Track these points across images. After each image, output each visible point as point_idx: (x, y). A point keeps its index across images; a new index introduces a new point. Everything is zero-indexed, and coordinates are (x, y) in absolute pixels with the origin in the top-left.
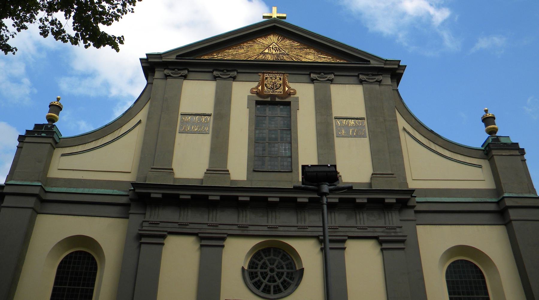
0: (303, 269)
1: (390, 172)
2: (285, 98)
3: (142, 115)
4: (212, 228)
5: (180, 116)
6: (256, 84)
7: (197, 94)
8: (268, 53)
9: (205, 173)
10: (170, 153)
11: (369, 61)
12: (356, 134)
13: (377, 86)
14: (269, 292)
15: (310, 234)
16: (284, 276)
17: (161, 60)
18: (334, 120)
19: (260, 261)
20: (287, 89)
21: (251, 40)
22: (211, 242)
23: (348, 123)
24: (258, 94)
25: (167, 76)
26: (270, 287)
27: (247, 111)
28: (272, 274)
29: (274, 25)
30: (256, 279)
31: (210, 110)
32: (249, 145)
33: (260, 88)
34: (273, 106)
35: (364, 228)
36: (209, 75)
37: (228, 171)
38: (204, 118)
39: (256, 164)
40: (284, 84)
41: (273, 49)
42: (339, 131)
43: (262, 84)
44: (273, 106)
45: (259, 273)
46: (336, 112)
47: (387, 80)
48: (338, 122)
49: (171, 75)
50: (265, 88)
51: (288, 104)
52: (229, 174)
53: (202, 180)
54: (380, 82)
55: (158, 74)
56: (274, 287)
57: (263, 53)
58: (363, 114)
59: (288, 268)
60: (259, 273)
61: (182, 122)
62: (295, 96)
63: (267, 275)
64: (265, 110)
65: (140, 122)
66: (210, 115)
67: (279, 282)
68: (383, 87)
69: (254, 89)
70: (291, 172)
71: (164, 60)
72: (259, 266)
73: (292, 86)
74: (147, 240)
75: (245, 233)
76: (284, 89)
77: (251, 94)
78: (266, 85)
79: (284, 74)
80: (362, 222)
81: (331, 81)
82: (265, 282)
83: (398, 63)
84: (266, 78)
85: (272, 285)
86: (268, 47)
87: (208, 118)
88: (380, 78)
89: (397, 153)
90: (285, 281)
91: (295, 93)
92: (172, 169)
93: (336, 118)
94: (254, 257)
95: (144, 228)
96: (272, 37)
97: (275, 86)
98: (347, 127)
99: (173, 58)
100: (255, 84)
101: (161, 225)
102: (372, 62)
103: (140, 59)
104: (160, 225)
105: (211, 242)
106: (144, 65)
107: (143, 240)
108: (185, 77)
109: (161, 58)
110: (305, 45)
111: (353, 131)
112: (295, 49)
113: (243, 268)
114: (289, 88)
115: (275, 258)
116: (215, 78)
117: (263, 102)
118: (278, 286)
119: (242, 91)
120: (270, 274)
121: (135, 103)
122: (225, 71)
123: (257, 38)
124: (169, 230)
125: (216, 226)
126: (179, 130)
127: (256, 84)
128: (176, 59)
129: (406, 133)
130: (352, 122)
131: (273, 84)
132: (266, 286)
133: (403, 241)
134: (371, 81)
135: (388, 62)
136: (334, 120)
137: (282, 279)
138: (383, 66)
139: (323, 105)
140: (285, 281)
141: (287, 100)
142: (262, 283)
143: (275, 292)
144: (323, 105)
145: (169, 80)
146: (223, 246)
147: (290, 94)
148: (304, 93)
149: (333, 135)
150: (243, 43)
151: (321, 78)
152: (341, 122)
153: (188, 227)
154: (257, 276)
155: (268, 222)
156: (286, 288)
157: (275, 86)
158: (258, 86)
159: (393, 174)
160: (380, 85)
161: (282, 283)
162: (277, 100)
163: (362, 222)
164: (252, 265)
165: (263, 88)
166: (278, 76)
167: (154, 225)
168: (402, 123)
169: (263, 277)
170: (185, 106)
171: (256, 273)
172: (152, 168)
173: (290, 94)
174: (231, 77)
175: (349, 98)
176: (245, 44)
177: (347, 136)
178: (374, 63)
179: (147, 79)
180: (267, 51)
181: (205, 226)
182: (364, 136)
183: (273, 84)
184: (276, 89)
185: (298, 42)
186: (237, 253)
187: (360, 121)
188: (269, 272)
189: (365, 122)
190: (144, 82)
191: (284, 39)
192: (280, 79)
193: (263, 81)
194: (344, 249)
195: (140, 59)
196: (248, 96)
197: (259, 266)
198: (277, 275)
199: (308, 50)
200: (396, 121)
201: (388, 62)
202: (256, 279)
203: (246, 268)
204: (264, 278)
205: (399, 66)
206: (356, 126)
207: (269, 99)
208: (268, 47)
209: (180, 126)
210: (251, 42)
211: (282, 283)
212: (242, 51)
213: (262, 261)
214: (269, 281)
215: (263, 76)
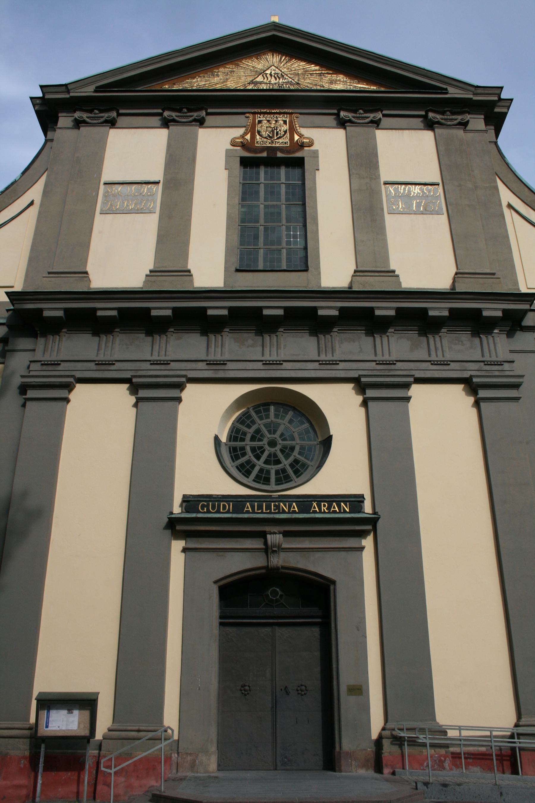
0: (331, 437)
1: (488, 271)
2: (294, 152)
3: (35, 193)
4: (158, 367)
5: (102, 187)
6: (242, 131)
7: (134, 150)
8: (261, 83)
9: (147, 276)
10: (84, 246)
11: (446, 89)
12: (425, 209)
13: (460, 133)
14: (267, 481)
15: (342, 374)
16: (296, 453)
17: (67, 96)
18: (383, 187)
19: (249, 427)
20: (296, 138)
21: (231, 63)
22: (155, 392)
23: (409, 191)
24: (243, 146)
25: (78, 124)
26: (268, 472)
27: (225, 174)
28: (273, 450)
29: (274, 35)
30: (243, 460)
31: (158, 175)
32: (228, 228)
33: (248, 137)
34: (273, 174)
35: (446, 363)
36: (156, 120)
37: (189, 271)
38: (146, 188)
39: (243, 260)
40: (292, 130)
41: (271, 75)
42: (393, 204)
43: (252, 130)
44: (273, 174)
45: (248, 449)
46: (386, 173)
47: (477, 122)
48: (391, 189)
49: (88, 120)
50: (258, 137)
51: (299, 163)
52: (192, 276)
53: (142, 288)
54: (464, 125)
55: (65, 120)
56: (277, 472)
58: (437, 179)
59: (302, 439)
60: (248, 449)
61: (106, 195)
62: (312, 148)
63: (263, 452)
64: (258, 174)
65: (32, 203)
66: (157, 183)
67: (286, 463)
68: (470, 135)
69: (238, 138)
70: (306, 270)
71: (72, 94)
72: (248, 437)
73: (307, 133)
75: (221, 375)
76: (292, 138)
77: (232, 148)
78: (259, 132)
79: (292, 113)
80: (440, 353)
81: (376, 123)
82: (260, 464)
83: (497, 91)
84: (260, 122)
85: (273, 469)
86: (262, 73)
87: (154, 187)
88: (467, 117)
89: (501, 241)
90: (296, 461)
91: (311, 144)
92: (86, 273)
93: (385, 183)
95: (32, 373)
96: (269, 57)
97: (274, 133)
98: (408, 197)
99: (89, 91)
100: (238, 132)
101: (63, 366)
102: (451, 90)
103: (31, 98)
104: (60, 368)
105: (155, 392)
106: (37, 108)
107: (31, 394)
108: (112, 123)
109: (68, 92)
110: (328, 68)
111: (418, 205)
112: (311, 74)
113: (217, 439)
114: (301, 136)
115: (279, 421)
116: (166, 124)
117: (252, 161)
118: (284, 471)
119: (215, 144)
120: (268, 451)
121: (23, 173)
122: (185, 110)
123: (243, 59)
124: (78, 375)
125: (167, 363)
126: (101, 210)
127: (242, 131)
128: (95, 91)
129: (513, 211)
130: (416, 190)
131: (273, 131)
132: (261, 470)
134: (449, 123)
135: (479, 91)
136: (383, 187)
137: (291, 459)
138: (471, 96)
139: (363, 164)
140: (296, 461)
141: (298, 155)
142: (254, 466)
143: (279, 482)
145: (84, 130)
147: (302, 146)
148: (328, 144)
149: (383, 209)
150: (218, 67)
151: (358, 118)
152: (396, 190)
153: (112, 367)
154: (244, 454)
155: (263, 355)
156: (297, 473)
157: (274, 133)
158: (245, 134)
159: (494, 274)
160: (465, 130)
161: (291, 465)
162: (279, 155)
163: (440, 353)
164: (235, 434)
165: (253, 137)
166: (281, 119)
167: (51, 368)
168: (506, 196)
169: (255, 456)
170: (110, 171)
171: (243, 448)
172: (49, 273)
173: (302, 146)
174: (195, 120)
175: (408, 152)
176: (222, 69)
177: (408, 212)
178: (453, 93)
179: (45, 135)
180: (260, 79)
181: (147, 366)
182: (439, 213)
183: (273, 131)
184: (278, 139)
185: (316, 65)
186: (206, 412)
187: (430, 187)
188: (267, 447)
189: (440, 189)
190: (42, 139)
191: (290, 61)
192: (285, 122)
193: (253, 126)
194: (408, 399)
195: (31, 98)
196: (227, 151)
197: (248, 437)
198: (282, 451)
199: (334, 77)
200: (496, 188)
201: (479, 91)
202: (243, 460)
203: (224, 439)
204: (258, 458)
205: (500, 99)
206: (424, 196)
207: (265, 154)
208: (262, 73)
209: (103, 203)
210: (231, 66)
211: (291, 465)
212: (216, 80)
213: (254, 428)
214: (266, 462)
215: (254, 119)
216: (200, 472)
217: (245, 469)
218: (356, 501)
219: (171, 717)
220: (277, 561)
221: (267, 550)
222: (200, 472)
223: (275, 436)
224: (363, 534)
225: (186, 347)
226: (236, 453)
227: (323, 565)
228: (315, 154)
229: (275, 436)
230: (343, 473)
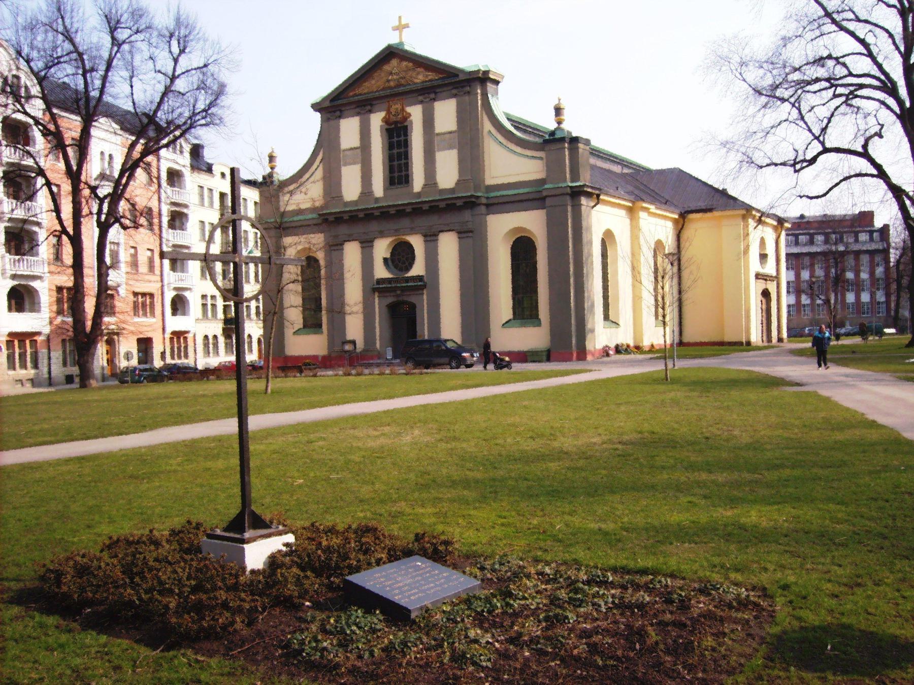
7: (349, 130)
22: (367, 245)
57: (388, 81)
74: (335, 247)
94: (393, 249)
99: (327, 104)
105: (367, 245)
113: (385, 260)
130: (447, 136)
133: (471, 232)
139: (429, 122)
144: (429, 122)
146: (372, 246)
175: (446, 113)
178: (462, 77)
186: (382, 248)
203: (388, 256)
212: (373, 82)
216: (381, 272)
217: (396, 267)
218: (420, 278)
219: (378, 345)
220: (400, 299)
221: (398, 296)
222: (381, 272)
223: (401, 256)
224: (423, 289)
225: (374, 226)
226: (393, 261)
227: (413, 299)
228: (411, 122)
229: (401, 256)
230: (418, 269)
